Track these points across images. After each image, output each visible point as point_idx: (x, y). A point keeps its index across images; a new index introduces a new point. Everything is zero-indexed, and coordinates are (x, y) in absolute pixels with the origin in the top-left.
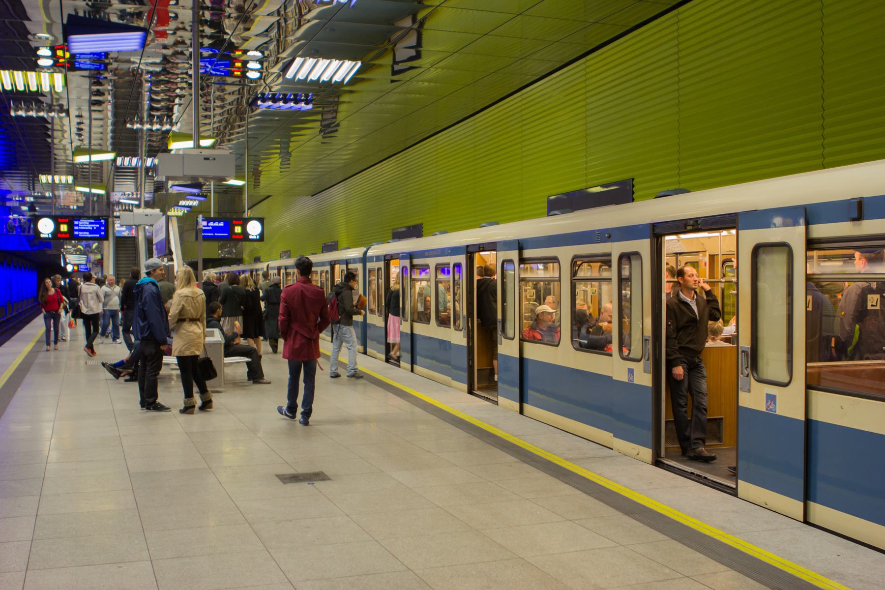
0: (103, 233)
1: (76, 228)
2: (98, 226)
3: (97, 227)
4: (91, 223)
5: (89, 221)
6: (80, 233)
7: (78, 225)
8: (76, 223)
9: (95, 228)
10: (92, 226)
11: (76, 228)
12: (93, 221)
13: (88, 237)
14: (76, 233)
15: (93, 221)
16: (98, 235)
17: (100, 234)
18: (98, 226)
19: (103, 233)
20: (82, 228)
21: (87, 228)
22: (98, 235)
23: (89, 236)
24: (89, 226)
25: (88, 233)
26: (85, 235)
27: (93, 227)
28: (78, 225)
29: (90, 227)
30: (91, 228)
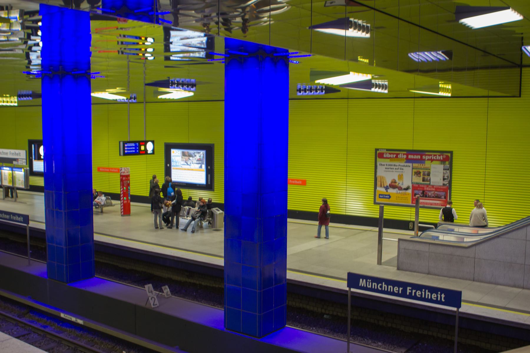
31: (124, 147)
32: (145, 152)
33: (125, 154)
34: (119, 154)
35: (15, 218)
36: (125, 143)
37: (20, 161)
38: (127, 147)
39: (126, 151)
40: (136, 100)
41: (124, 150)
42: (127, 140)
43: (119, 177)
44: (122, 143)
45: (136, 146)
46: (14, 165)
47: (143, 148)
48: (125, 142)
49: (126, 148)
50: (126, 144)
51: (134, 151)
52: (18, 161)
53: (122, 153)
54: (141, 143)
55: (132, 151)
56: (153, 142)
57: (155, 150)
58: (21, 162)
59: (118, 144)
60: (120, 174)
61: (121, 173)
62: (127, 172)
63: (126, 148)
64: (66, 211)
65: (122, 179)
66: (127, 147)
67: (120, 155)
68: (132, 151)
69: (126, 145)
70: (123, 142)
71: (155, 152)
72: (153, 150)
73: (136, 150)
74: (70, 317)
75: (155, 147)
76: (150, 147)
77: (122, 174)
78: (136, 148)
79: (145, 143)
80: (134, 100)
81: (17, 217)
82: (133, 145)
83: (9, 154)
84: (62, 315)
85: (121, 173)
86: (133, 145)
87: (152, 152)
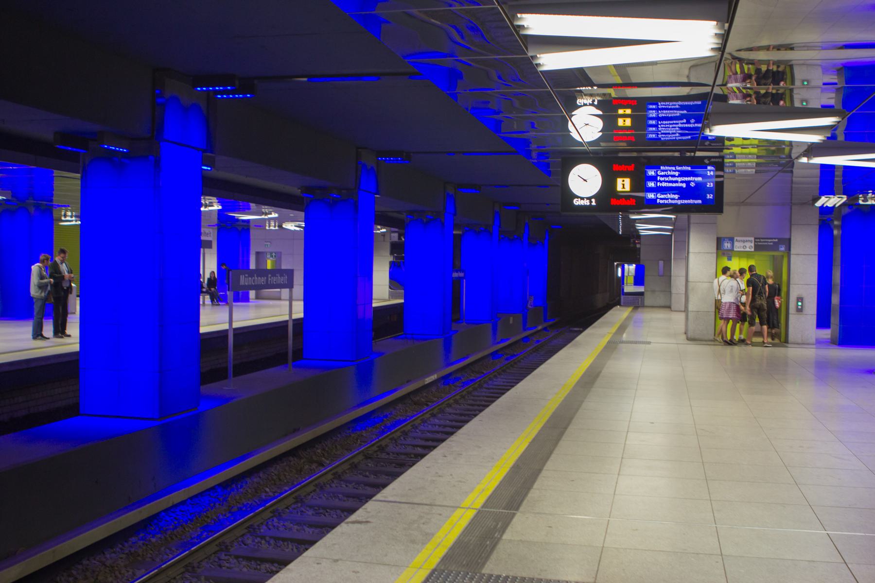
1: (651, 184)
4: (683, 174)
5: (678, 168)
6: (659, 196)
7: (653, 179)
8: (651, 173)
9: (692, 185)
10: (686, 179)
11: (651, 184)
12: (689, 169)
13: (676, 204)
15: (689, 169)
16: (700, 202)
20: (664, 184)
21: (674, 185)
22: (700, 202)
23: (679, 202)
24: (679, 179)
25: (676, 197)
27: (688, 183)
28: (653, 179)
30: (684, 185)
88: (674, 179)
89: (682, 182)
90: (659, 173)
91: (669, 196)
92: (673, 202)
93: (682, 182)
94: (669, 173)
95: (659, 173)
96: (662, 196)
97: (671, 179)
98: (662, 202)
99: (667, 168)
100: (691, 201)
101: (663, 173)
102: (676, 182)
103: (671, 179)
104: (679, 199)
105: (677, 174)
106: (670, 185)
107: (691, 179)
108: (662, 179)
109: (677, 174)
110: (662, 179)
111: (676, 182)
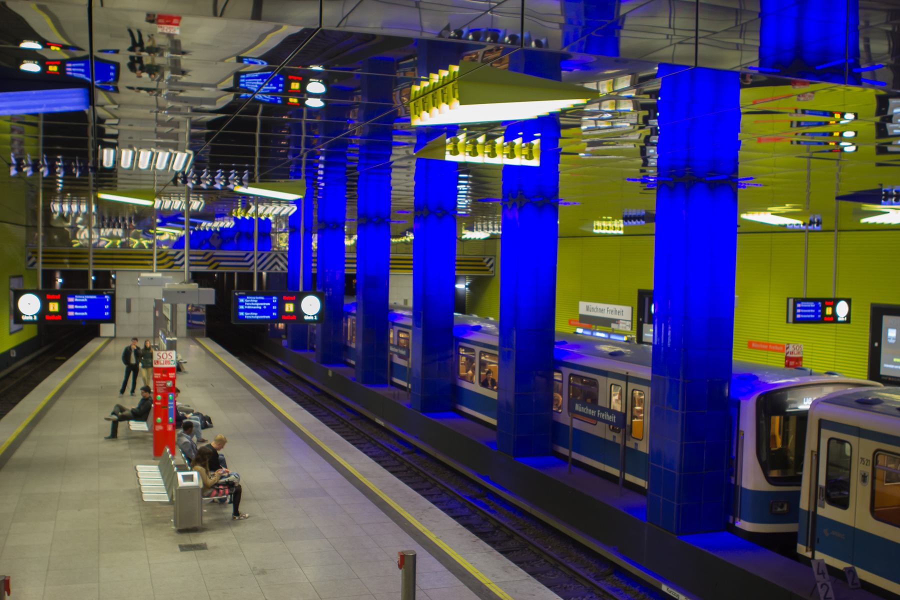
0: (274, 314)
1: (242, 307)
2: (269, 304)
3: (267, 306)
4: (260, 301)
5: (257, 298)
6: (246, 314)
7: (243, 304)
8: (242, 300)
9: (265, 307)
10: (261, 304)
11: (242, 307)
13: (256, 319)
14: (241, 314)
15: (263, 298)
16: (269, 317)
17: (271, 315)
18: (269, 304)
19: (274, 314)
20: (249, 307)
21: (255, 308)
22: (269, 317)
23: (258, 317)
24: (258, 304)
25: (256, 314)
26: (253, 317)
27: (262, 306)
28: (243, 304)
29: (258, 306)
30: (260, 308)
31: (795, 308)
32: (834, 318)
33: (796, 321)
34: (785, 320)
35: (603, 415)
36: (797, 301)
37: (623, 323)
38: (801, 308)
39: (798, 316)
40: (820, 226)
41: (795, 313)
42: (801, 295)
43: (784, 360)
44: (791, 301)
45: (816, 308)
46: (613, 329)
47: (829, 311)
48: (797, 299)
49: (799, 311)
50: (800, 302)
51: (812, 316)
52: (618, 324)
53: (791, 319)
54: (827, 303)
55: (809, 316)
56: (849, 301)
57: (852, 316)
58: (624, 325)
59: (786, 302)
60: (785, 354)
61: (787, 353)
62: (799, 353)
63: (799, 311)
64: (685, 412)
65: (789, 363)
66: (801, 308)
67: (787, 322)
68: (809, 316)
69: (799, 305)
70: (794, 299)
71: (852, 320)
72: (849, 316)
73: (816, 314)
74: (677, 593)
75: (852, 310)
76: (842, 309)
77: (789, 355)
78: (816, 311)
79: (834, 302)
80: (817, 225)
81: (608, 415)
82: (812, 305)
83: (606, 311)
84: (664, 588)
85: (787, 353)
86: (812, 305)
87: (846, 319)
88: (254, 304)
89: (259, 306)
90: (246, 301)
91: (252, 314)
92: (254, 317)
93: (259, 306)
94: (252, 301)
95: (246, 301)
96: (248, 314)
97: (253, 304)
98: (247, 317)
99: (250, 298)
100: (264, 317)
101: (248, 301)
102: (256, 306)
103: (253, 304)
104: (258, 315)
105: (256, 301)
106: (252, 307)
107: (264, 304)
108: (248, 304)
109: (256, 301)
110: (248, 304)
111: (256, 306)
